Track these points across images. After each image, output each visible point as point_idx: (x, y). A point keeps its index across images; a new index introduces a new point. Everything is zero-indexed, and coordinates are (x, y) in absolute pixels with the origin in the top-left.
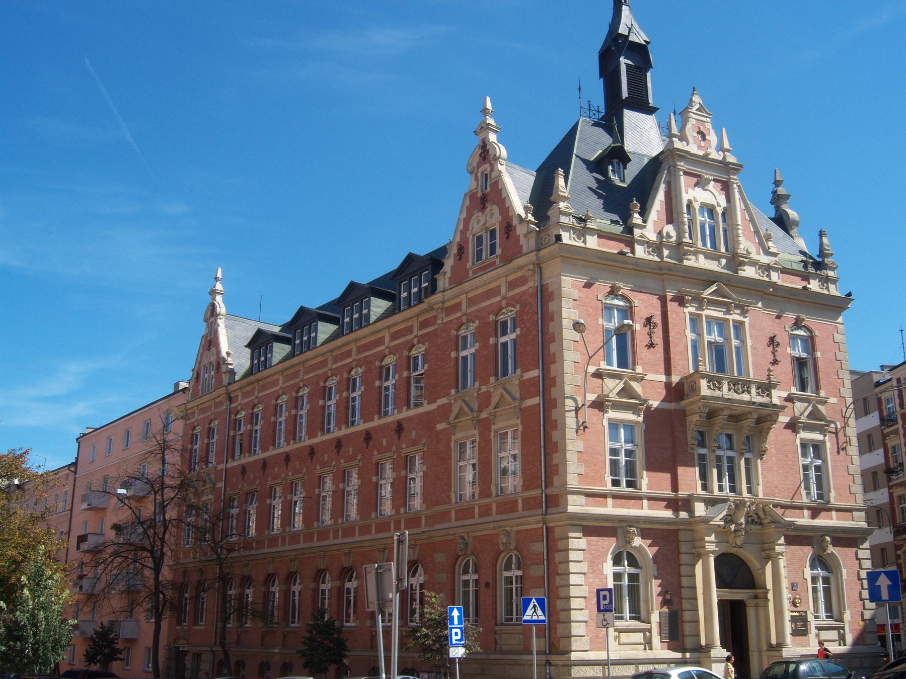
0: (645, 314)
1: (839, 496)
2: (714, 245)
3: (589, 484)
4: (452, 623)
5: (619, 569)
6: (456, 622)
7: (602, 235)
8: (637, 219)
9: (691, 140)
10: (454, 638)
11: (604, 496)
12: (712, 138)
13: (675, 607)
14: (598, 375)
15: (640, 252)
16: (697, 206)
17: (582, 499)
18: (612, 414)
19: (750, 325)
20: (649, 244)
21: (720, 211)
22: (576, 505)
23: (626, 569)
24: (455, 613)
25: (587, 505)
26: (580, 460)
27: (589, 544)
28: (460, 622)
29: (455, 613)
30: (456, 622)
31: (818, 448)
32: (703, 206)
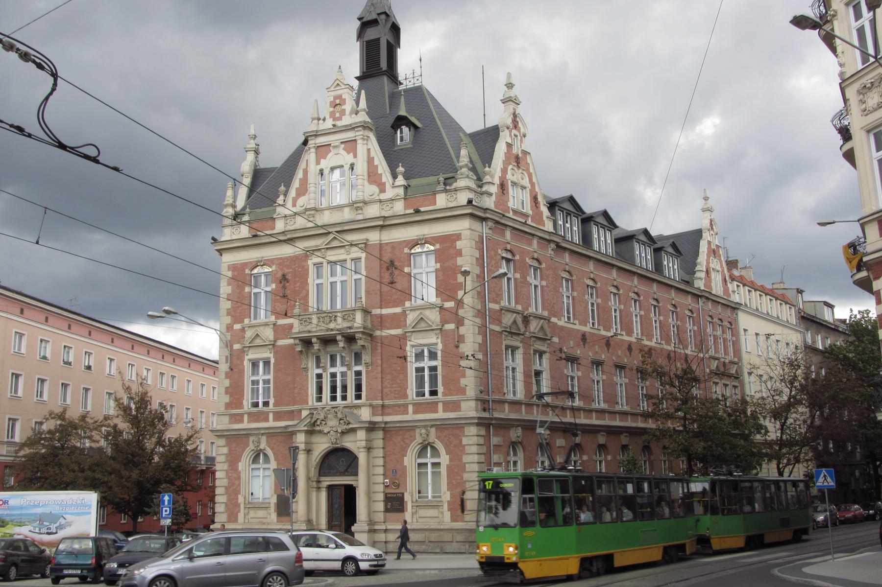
0: (279, 275)
4: (164, 503)
6: (166, 503)
8: (280, 200)
10: (164, 513)
11: (242, 415)
14: (243, 330)
15: (280, 226)
16: (326, 172)
18: (252, 355)
24: (166, 498)
25: (230, 423)
26: (227, 393)
27: (230, 450)
28: (169, 503)
29: (166, 498)
30: (166, 503)
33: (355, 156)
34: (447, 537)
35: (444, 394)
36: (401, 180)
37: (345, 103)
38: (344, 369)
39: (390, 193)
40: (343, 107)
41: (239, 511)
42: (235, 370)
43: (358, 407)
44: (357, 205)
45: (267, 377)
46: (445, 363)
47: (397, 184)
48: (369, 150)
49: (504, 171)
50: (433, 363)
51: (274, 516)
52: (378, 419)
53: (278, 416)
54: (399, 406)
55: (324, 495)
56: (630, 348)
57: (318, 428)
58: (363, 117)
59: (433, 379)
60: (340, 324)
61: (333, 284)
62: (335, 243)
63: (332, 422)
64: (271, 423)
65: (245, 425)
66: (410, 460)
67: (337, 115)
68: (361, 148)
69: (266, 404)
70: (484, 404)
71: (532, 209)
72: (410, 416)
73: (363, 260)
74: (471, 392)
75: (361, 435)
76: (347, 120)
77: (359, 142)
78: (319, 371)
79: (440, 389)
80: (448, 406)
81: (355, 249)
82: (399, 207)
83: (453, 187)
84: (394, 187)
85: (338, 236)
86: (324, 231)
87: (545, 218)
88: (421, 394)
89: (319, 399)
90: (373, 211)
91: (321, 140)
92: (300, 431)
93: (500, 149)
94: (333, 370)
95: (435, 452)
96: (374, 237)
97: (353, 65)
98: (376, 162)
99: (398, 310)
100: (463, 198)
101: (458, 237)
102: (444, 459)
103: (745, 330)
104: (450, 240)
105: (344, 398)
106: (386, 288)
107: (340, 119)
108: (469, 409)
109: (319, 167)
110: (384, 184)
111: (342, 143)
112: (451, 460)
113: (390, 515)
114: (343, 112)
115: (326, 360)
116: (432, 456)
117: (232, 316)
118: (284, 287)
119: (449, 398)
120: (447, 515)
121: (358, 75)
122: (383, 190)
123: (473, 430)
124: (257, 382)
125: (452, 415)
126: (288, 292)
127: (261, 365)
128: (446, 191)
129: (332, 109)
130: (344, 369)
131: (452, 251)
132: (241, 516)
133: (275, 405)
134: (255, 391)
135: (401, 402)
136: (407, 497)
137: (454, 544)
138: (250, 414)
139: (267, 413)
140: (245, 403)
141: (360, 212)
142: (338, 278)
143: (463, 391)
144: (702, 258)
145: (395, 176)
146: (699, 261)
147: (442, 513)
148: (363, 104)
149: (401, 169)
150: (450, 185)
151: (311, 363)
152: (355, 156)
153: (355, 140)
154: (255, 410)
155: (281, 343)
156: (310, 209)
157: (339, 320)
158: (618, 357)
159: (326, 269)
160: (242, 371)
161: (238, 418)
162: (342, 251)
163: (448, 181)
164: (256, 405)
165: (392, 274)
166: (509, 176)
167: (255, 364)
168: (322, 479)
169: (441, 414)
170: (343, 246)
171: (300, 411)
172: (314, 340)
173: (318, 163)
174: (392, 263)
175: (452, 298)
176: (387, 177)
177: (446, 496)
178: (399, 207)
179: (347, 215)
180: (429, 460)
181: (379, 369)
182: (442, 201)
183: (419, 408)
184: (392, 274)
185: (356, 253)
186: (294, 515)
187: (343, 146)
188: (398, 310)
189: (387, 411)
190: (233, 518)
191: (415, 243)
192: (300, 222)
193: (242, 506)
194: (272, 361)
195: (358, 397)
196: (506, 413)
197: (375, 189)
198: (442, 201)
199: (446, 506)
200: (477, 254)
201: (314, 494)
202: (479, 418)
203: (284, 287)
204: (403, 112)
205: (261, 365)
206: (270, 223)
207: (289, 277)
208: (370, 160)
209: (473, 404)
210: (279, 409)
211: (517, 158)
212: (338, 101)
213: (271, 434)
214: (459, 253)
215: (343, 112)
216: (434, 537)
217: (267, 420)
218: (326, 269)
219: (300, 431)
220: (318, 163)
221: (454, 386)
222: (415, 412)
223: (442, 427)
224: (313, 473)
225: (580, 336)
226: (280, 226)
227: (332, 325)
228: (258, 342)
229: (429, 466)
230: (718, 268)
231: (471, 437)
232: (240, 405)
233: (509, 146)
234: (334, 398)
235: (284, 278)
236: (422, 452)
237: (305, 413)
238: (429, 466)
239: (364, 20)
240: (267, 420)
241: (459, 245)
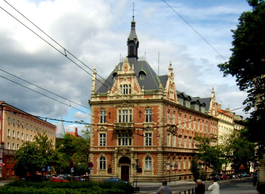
0: (108, 112)
1: (154, 144)
2: (127, 93)
3: (95, 146)
5: (101, 160)
7: (99, 97)
9: (123, 70)
11: (97, 148)
12: (129, 68)
13: (111, 167)
16: (122, 85)
17: (93, 148)
19: (133, 110)
20: (110, 97)
21: (128, 85)
22: (92, 150)
23: (103, 160)
25: (94, 149)
27: (94, 156)
32: (124, 86)
33: (131, 82)
34: (153, 178)
35: (153, 145)
36: (143, 90)
37: (128, 67)
38: (126, 138)
39: (140, 93)
40: (127, 68)
41: (97, 171)
42: (95, 136)
43: (131, 147)
44: (131, 96)
45: (104, 138)
46: (154, 137)
47: (142, 91)
48: (135, 81)
49: (169, 89)
50: (150, 137)
51: (107, 173)
52: (136, 150)
53: (108, 148)
54: (141, 147)
55: (120, 168)
56: (193, 132)
57: (120, 152)
58: (132, 72)
60: (127, 126)
61: (124, 116)
62: (125, 106)
63: (124, 151)
64: (106, 150)
65: (99, 150)
66: (144, 160)
67: (126, 70)
68: (133, 80)
69: (104, 145)
70: (163, 148)
71: (174, 98)
72: (144, 150)
73: (132, 110)
75: (132, 155)
76: (128, 72)
77: (132, 79)
78: (120, 138)
79: (152, 144)
81: (131, 107)
83: (157, 94)
84: (141, 92)
85: (126, 104)
86: (121, 102)
87: (177, 100)
88: (147, 145)
89: (120, 145)
90: (135, 98)
91: (121, 77)
92: (116, 153)
93: (168, 82)
94: (123, 138)
95: (150, 159)
96: (136, 105)
97: (125, 53)
98: (137, 84)
99: (142, 124)
101: (158, 106)
103: (220, 126)
105: (126, 145)
106: (138, 118)
107: (126, 71)
109: (120, 84)
110: (139, 91)
111: (127, 78)
112: (154, 161)
113: (138, 173)
114: (127, 70)
115: (122, 135)
116: (149, 159)
117: (95, 122)
118: (110, 115)
119: (155, 146)
120: (153, 173)
121: (127, 56)
122: (138, 92)
123: (160, 154)
124: (102, 139)
125: (155, 150)
126: (111, 117)
127: (103, 135)
128: (155, 95)
129: (124, 68)
130: (126, 138)
131: (157, 110)
132: (97, 173)
133: (107, 145)
134: (101, 142)
135: (142, 146)
136: (143, 169)
137: (155, 180)
138: (100, 148)
139: (105, 147)
140: (98, 144)
141: (132, 97)
142: (125, 114)
143: (158, 144)
144: (211, 106)
145: (141, 89)
146: (210, 107)
147: (152, 173)
148: (133, 68)
149: (143, 87)
150: (157, 93)
151: (118, 136)
152: (131, 82)
153: (131, 78)
154: (101, 146)
155: (108, 130)
156: (118, 95)
157: (127, 125)
158: (190, 135)
159: (122, 112)
160: (98, 136)
161: (97, 148)
162: (127, 107)
163: (156, 92)
164: (101, 145)
165: (140, 115)
166: (170, 90)
167: (101, 135)
168: (120, 164)
169: (152, 150)
170: (127, 106)
171: (114, 148)
172: (120, 130)
173: (120, 83)
174: (140, 112)
176: (139, 89)
177: (153, 169)
178: (143, 98)
179: (128, 98)
180: (148, 160)
181: (136, 138)
183: (146, 148)
184: (140, 115)
185: (130, 108)
186: (113, 173)
187: (127, 79)
188: (142, 124)
189: (138, 148)
190: (95, 173)
192: (115, 99)
193: (98, 170)
194: (106, 134)
195: (130, 144)
196: (167, 150)
197: (136, 92)
199: (153, 171)
200: (162, 111)
201: (118, 168)
202: (162, 152)
203: (110, 115)
204: (142, 70)
205: (103, 135)
206: (105, 98)
207: (111, 113)
208: (135, 84)
209: (160, 148)
210: (108, 146)
211: (172, 85)
212: (126, 66)
213: (106, 153)
214: (158, 110)
215: (127, 70)
216: (149, 178)
217: (105, 149)
218: (122, 112)
219: (116, 153)
220: (120, 83)
221: (156, 143)
222: (145, 149)
223: (152, 153)
224: (118, 163)
225: (182, 130)
226: (109, 99)
227: (125, 127)
228: (102, 129)
229: (148, 162)
230: (215, 109)
232: (97, 145)
233: (170, 82)
234: (123, 145)
235: (110, 113)
236: (147, 159)
237: (116, 149)
238: (148, 162)
239: (130, 40)
240: (105, 149)
241: (159, 108)
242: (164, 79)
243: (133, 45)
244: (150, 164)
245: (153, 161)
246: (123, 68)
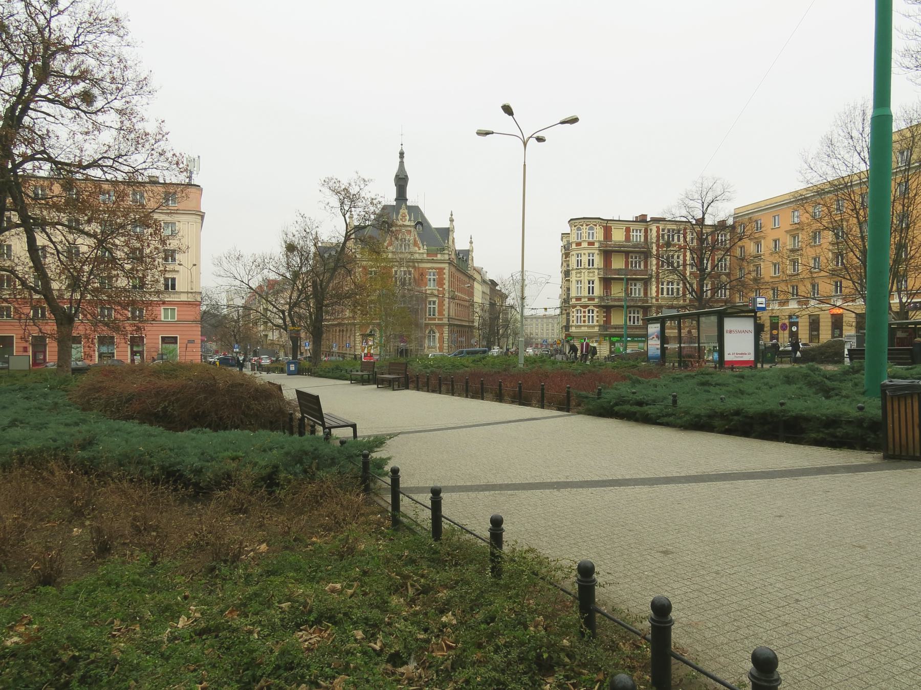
12: (408, 218)
31: (434, 303)
39: (421, 251)
59: (434, 311)
68: (412, 234)
74: (446, 316)
80: (439, 319)
82: (425, 256)
95: (434, 333)
100: (447, 257)
102: (437, 335)
104: (442, 269)
108: (445, 321)
169: (437, 322)
175: (442, 287)
176: (421, 245)
182: (439, 256)
183: (430, 319)
191: (429, 268)
198: (439, 256)
223: (437, 325)
231: (446, 329)
242: (446, 233)
243: (401, 181)
244: (434, 339)
245: (437, 335)
246: (400, 217)
